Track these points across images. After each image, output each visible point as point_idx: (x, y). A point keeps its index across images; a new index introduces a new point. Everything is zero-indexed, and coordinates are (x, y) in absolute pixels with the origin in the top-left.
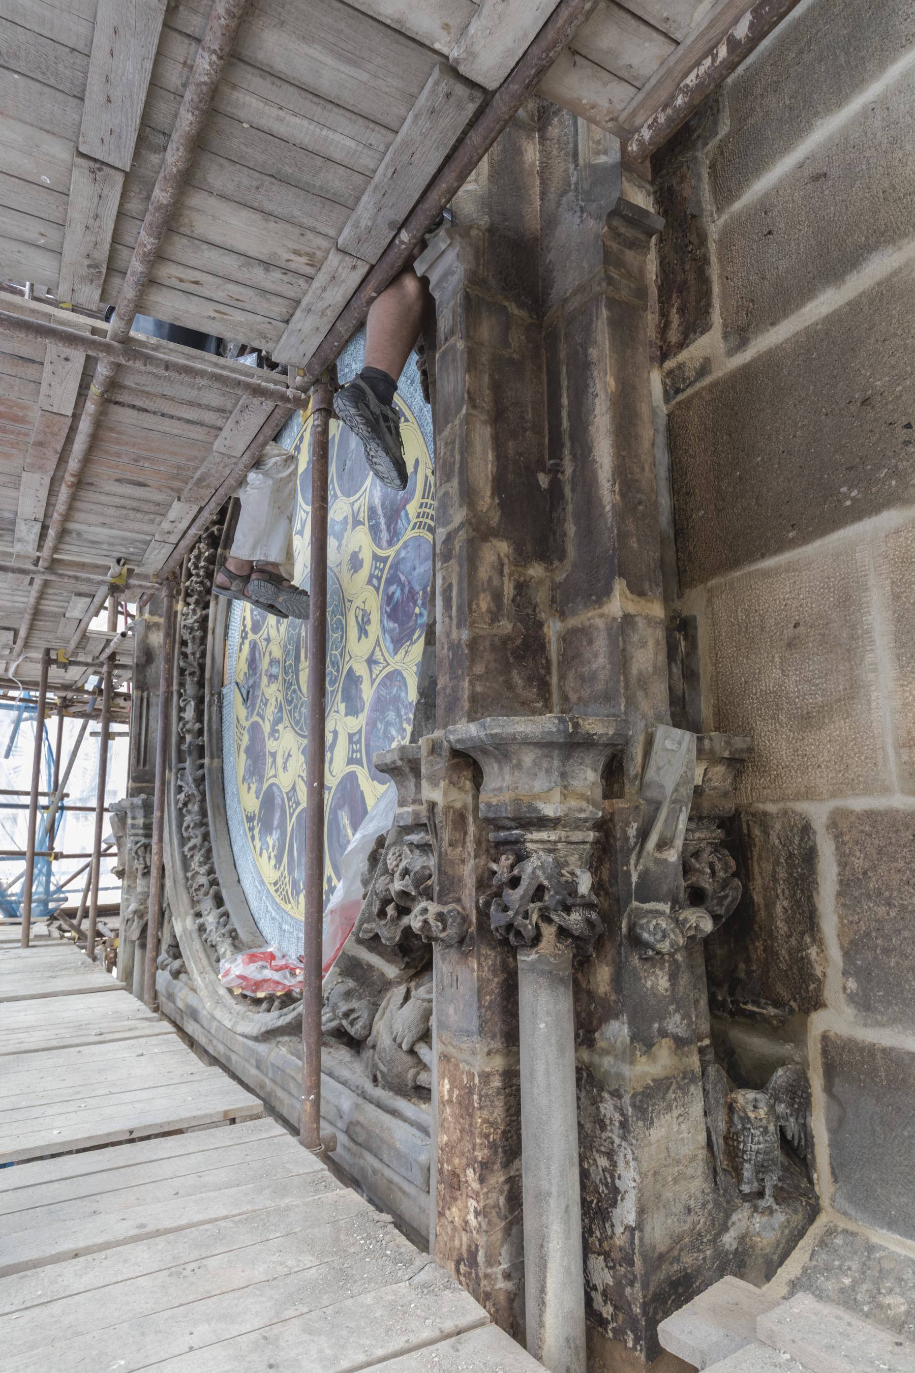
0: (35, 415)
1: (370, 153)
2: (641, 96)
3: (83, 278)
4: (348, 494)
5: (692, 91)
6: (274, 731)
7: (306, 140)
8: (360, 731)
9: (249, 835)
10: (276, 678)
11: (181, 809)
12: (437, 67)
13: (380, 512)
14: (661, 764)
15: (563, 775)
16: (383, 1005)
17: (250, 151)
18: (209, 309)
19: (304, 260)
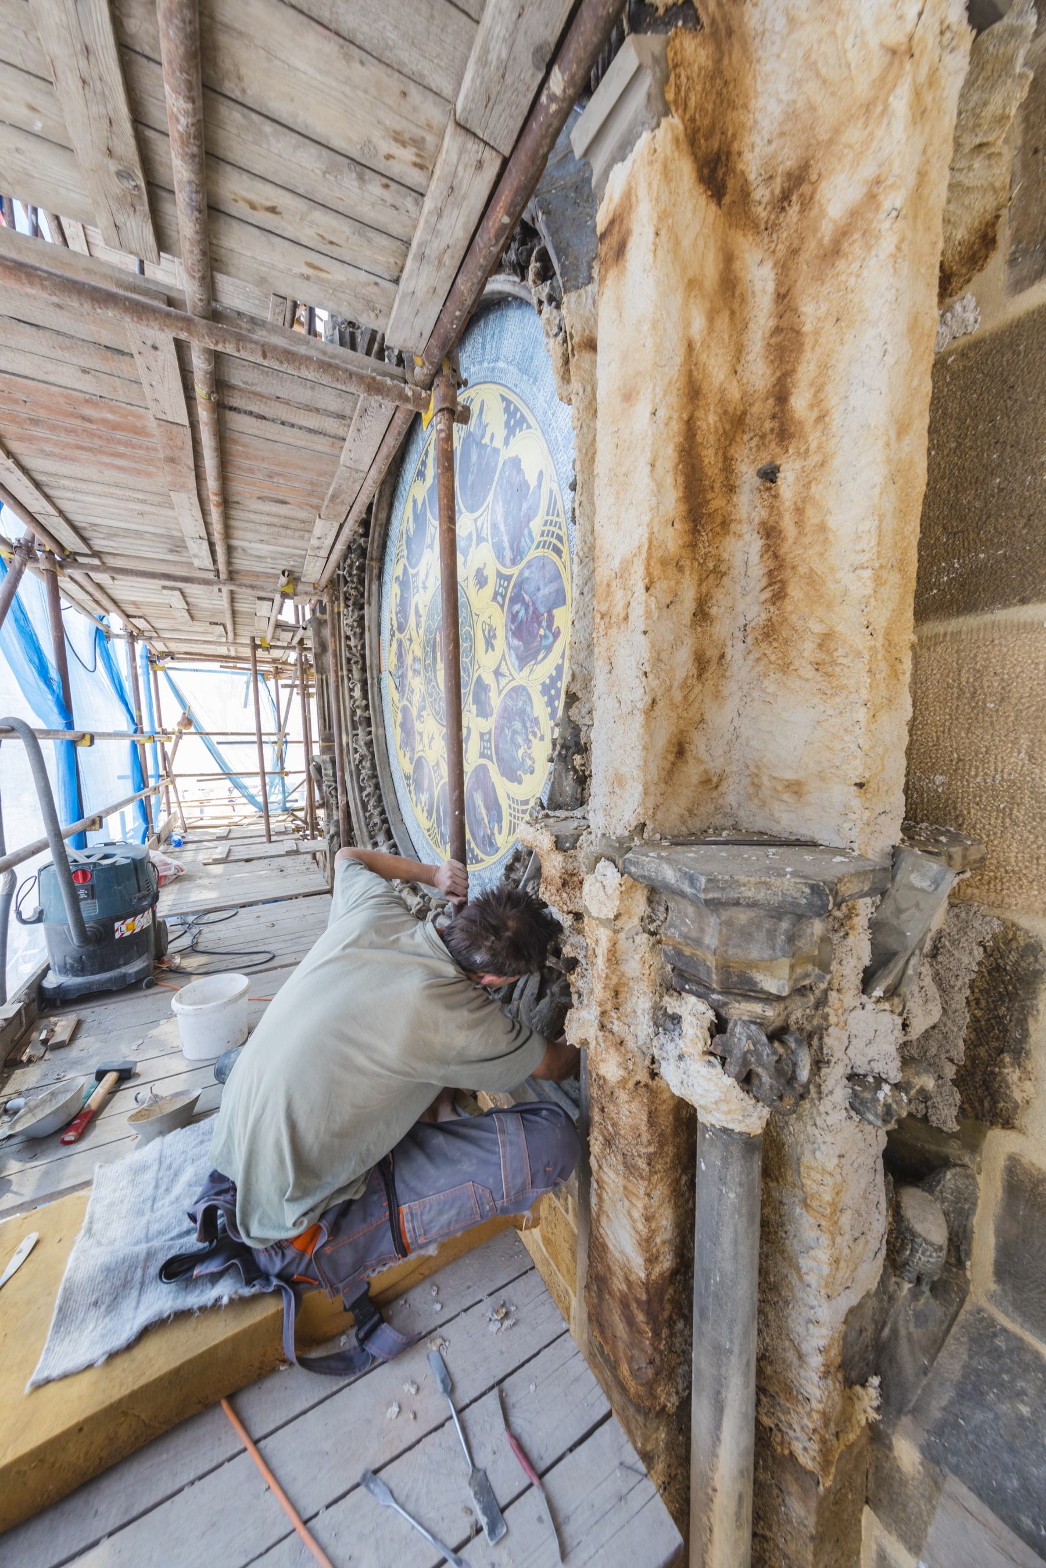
0: (152, 425)
6: (420, 716)
8: (490, 733)
14: (904, 906)
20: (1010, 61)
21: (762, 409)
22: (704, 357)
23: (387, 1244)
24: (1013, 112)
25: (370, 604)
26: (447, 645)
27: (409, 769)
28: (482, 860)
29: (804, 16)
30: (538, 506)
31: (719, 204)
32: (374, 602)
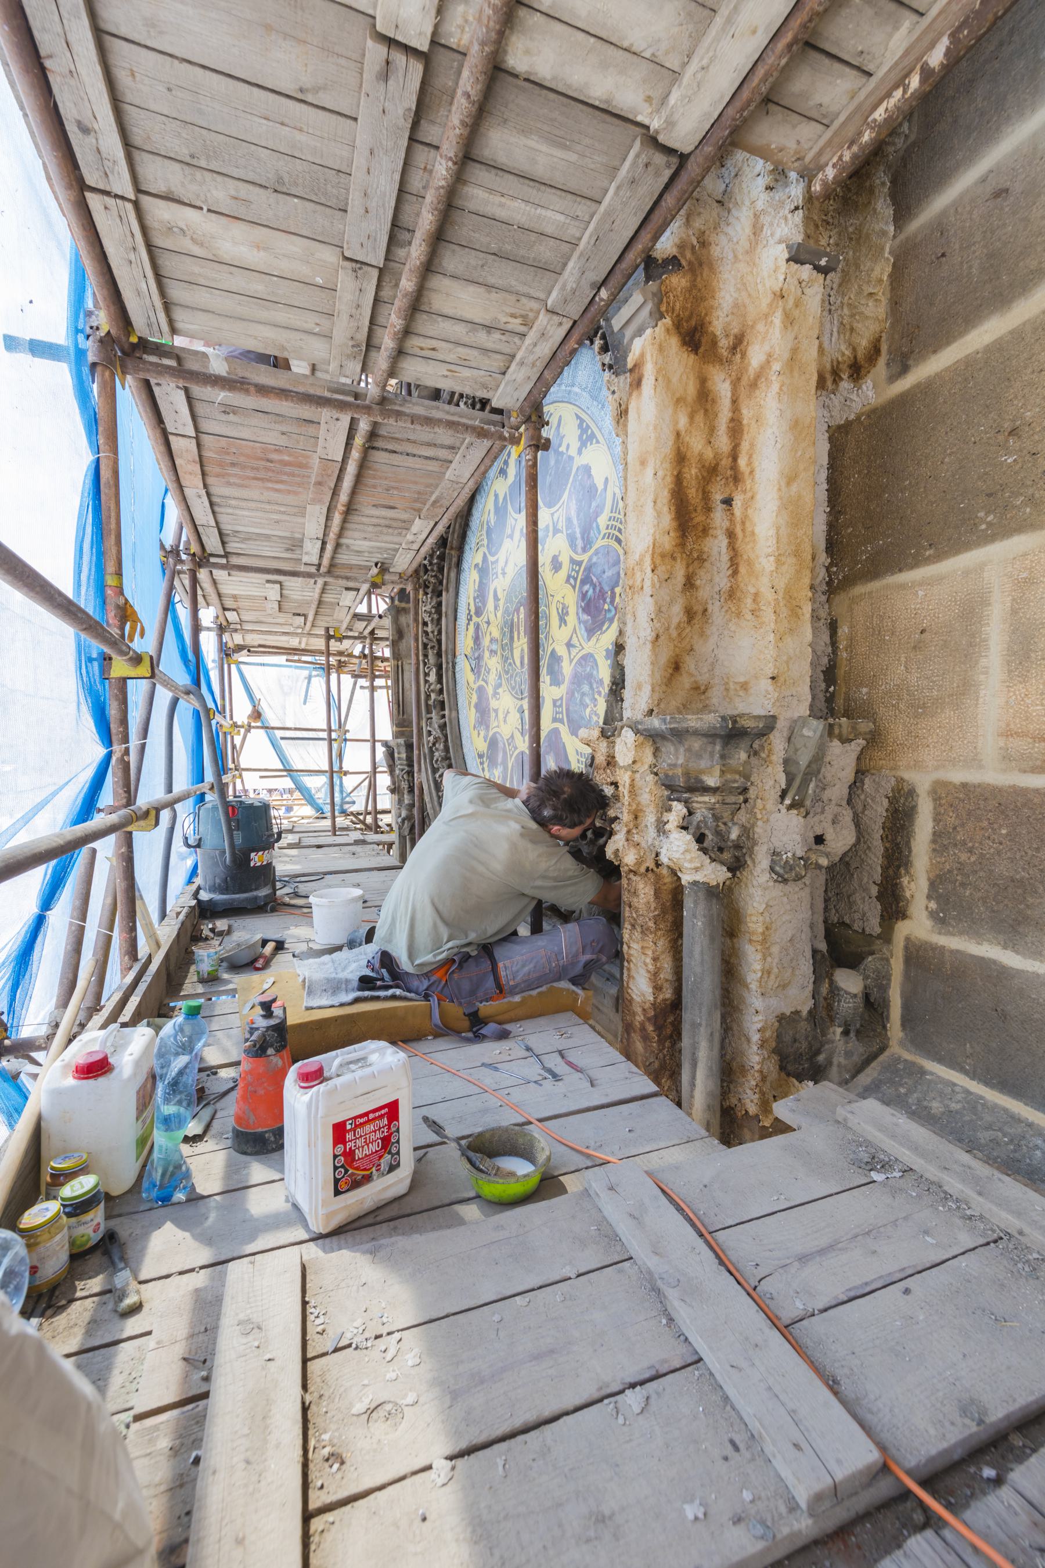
0: (315, 462)
1: (577, 223)
2: (829, 133)
3: (348, 356)
4: (550, 505)
5: (880, 126)
6: (495, 694)
8: (561, 698)
9: (480, 767)
10: (496, 653)
11: (431, 748)
12: (639, 139)
13: (575, 522)
14: (798, 746)
15: (723, 757)
17: (477, 235)
18: (443, 369)
19: (519, 321)
20: (883, 249)
21: (726, 462)
22: (687, 439)
23: (490, 983)
24: (885, 278)
25: (447, 591)
26: (530, 616)
27: (482, 746)
29: (740, 257)
30: (604, 505)
31: (697, 354)
32: (452, 589)
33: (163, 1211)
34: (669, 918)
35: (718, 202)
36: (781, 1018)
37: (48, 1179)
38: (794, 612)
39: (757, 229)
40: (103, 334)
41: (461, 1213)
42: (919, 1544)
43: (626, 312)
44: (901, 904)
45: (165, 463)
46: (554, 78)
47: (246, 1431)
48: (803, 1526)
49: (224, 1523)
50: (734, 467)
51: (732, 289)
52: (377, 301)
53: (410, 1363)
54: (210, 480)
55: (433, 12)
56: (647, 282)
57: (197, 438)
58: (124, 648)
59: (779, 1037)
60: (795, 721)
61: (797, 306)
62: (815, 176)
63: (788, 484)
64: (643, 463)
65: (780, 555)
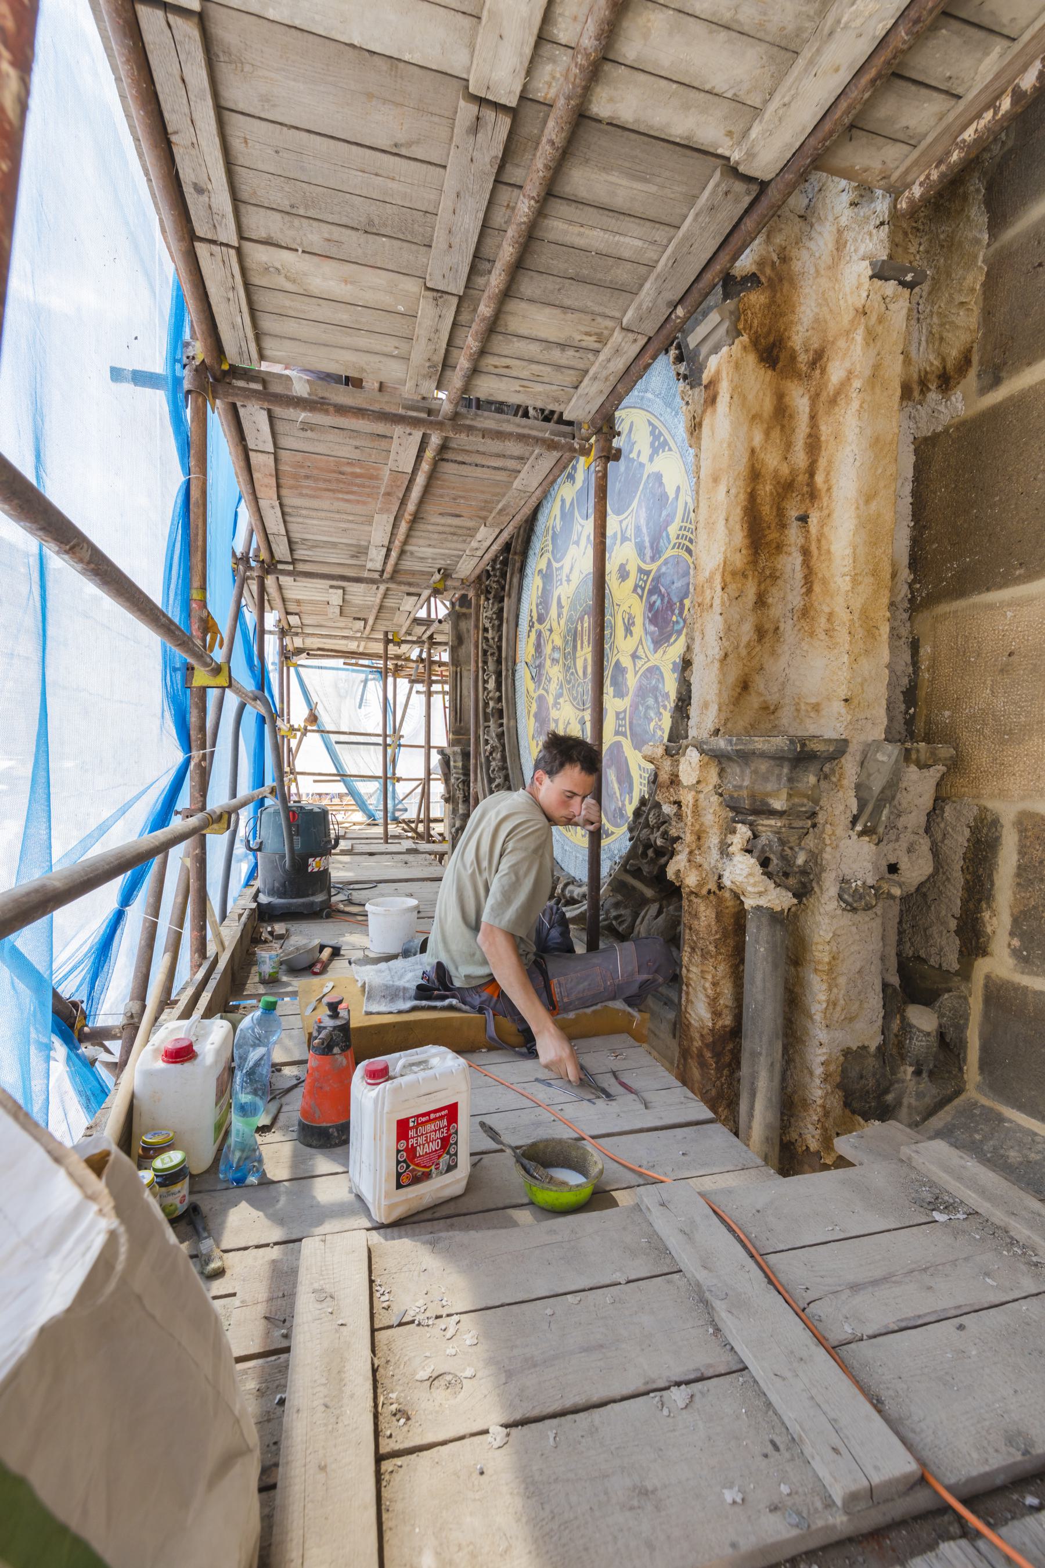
0: (386, 474)
1: (655, 248)
2: (916, 154)
5: (969, 147)
6: (556, 703)
7: (601, 247)
8: (625, 711)
10: (558, 661)
11: (488, 757)
12: (719, 170)
13: (644, 530)
14: (871, 771)
15: (790, 780)
16: (642, 914)
17: (555, 262)
18: (516, 385)
19: (593, 338)
20: (976, 257)
21: (802, 478)
24: (978, 287)
25: (509, 596)
26: (595, 628)
28: (613, 833)
29: (822, 272)
30: (675, 514)
31: (774, 370)
32: (514, 594)
33: (238, 1191)
34: (731, 942)
35: (800, 217)
36: (847, 1053)
37: (140, 1152)
38: (871, 632)
39: (840, 245)
40: (198, 363)
41: (515, 1217)
42: (951, 1550)
43: (701, 331)
44: (982, 940)
45: (243, 477)
46: (637, 121)
47: (324, 1381)
48: (839, 1521)
49: (308, 1452)
50: (811, 483)
51: (813, 304)
52: (455, 324)
53: (468, 1342)
54: (284, 492)
55: (523, 74)
56: (725, 299)
57: (275, 454)
58: (208, 660)
59: (844, 1072)
60: (869, 745)
61: (880, 322)
62: (902, 192)
63: (867, 502)
64: (716, 480)
65: (856, 574)
